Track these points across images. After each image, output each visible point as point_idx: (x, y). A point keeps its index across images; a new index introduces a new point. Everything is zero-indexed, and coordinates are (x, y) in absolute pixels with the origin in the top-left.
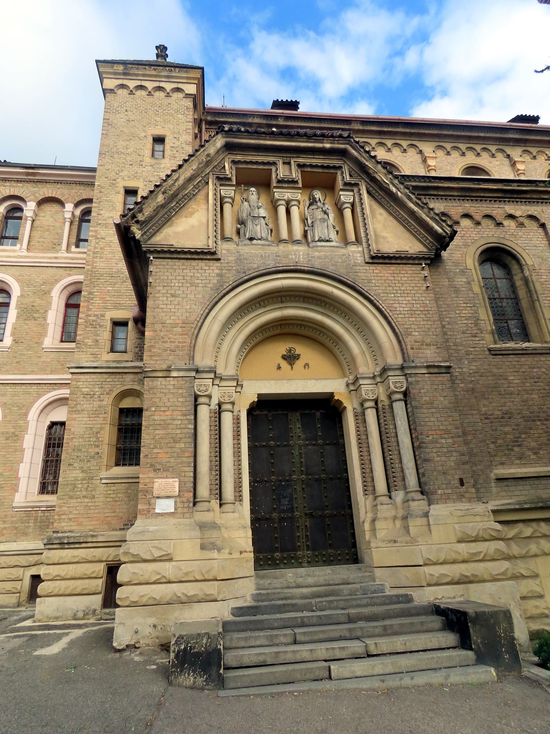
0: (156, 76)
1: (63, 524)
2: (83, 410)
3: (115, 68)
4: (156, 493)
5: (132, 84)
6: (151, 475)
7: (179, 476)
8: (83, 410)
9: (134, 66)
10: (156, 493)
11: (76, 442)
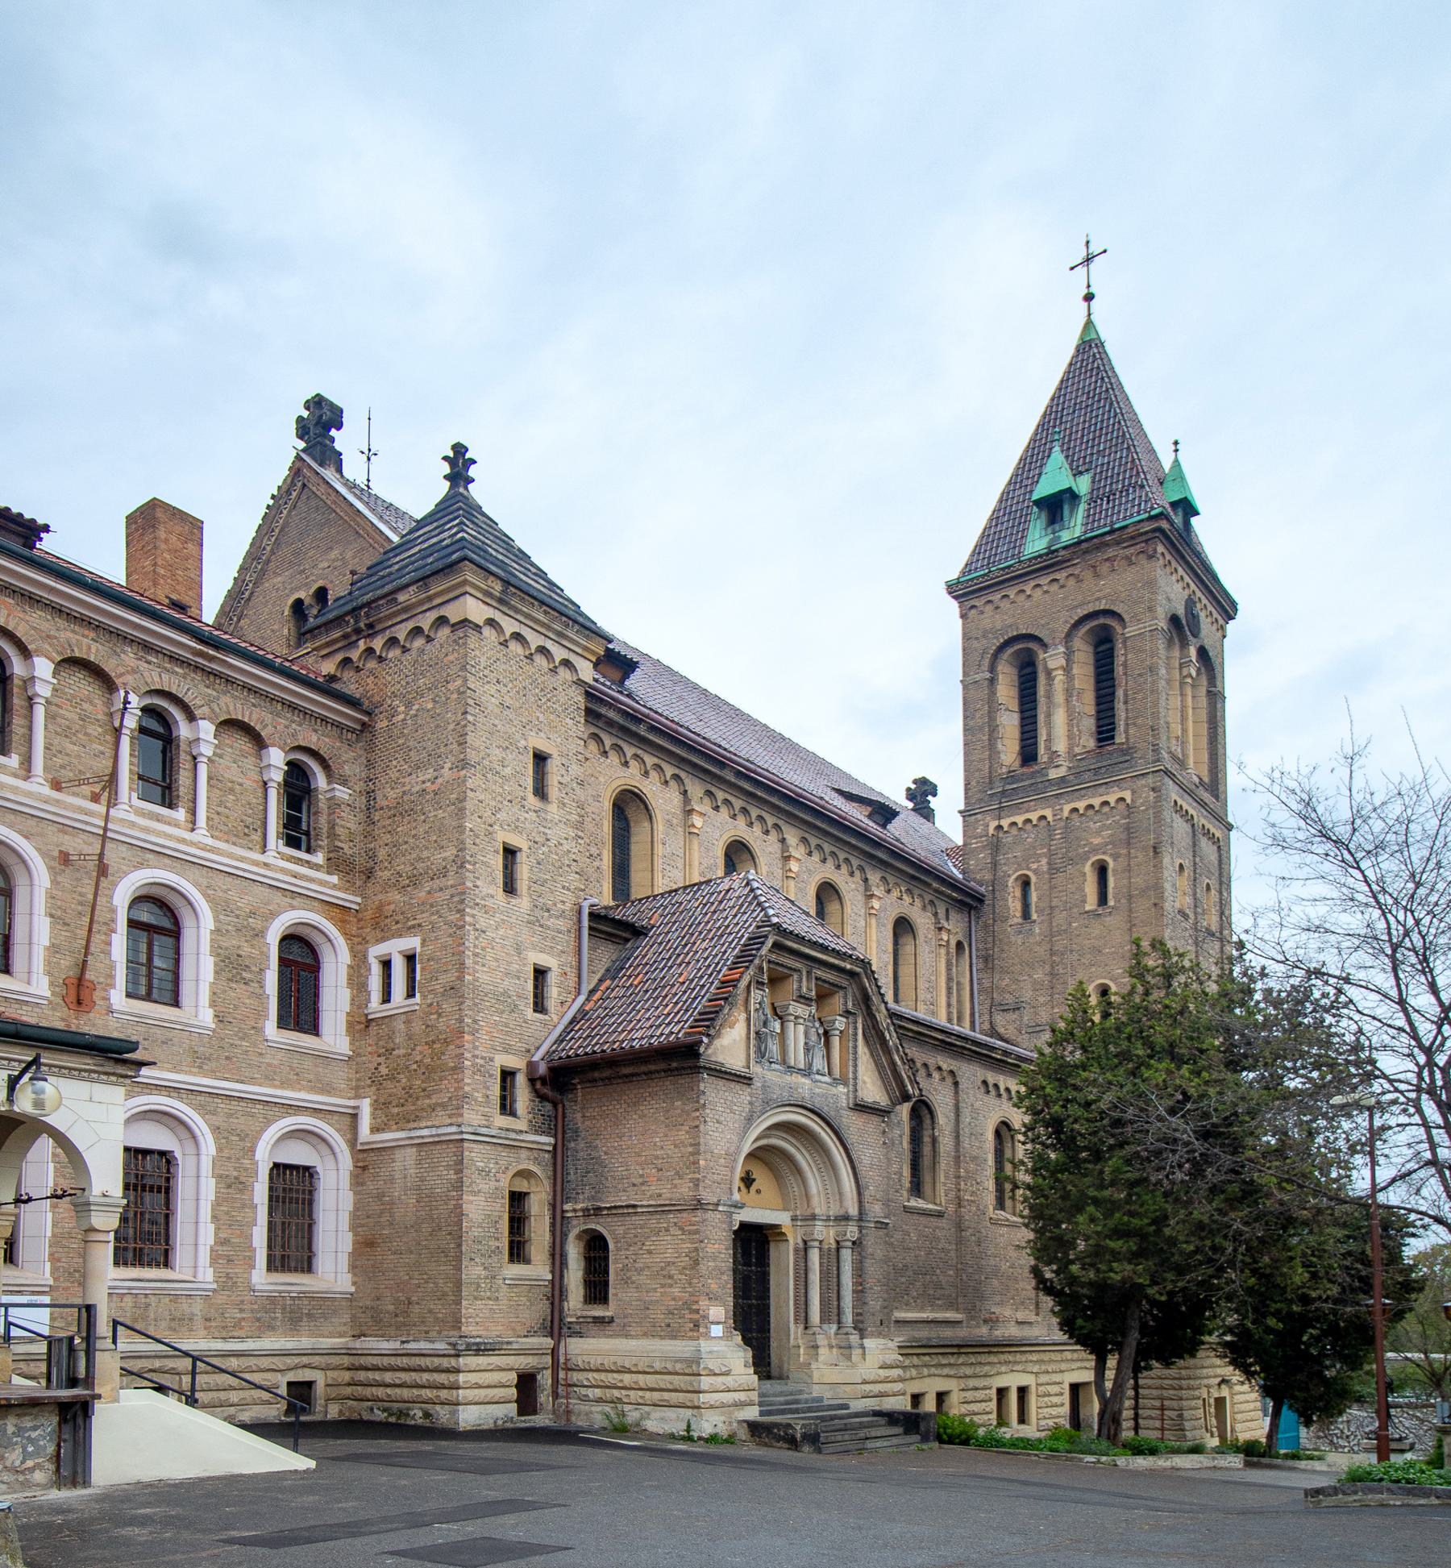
0: (543, 624)
1: (470, 1328)
2: (479, 1191)
3: (489, 583)
4: (711, 1319)
5: (509, 626)
6: (707, 1303)
7: (724, 1305)
8: (479, 1191)
9: (518, 593)
10: (711, 1319)
11: (475, 1232)
